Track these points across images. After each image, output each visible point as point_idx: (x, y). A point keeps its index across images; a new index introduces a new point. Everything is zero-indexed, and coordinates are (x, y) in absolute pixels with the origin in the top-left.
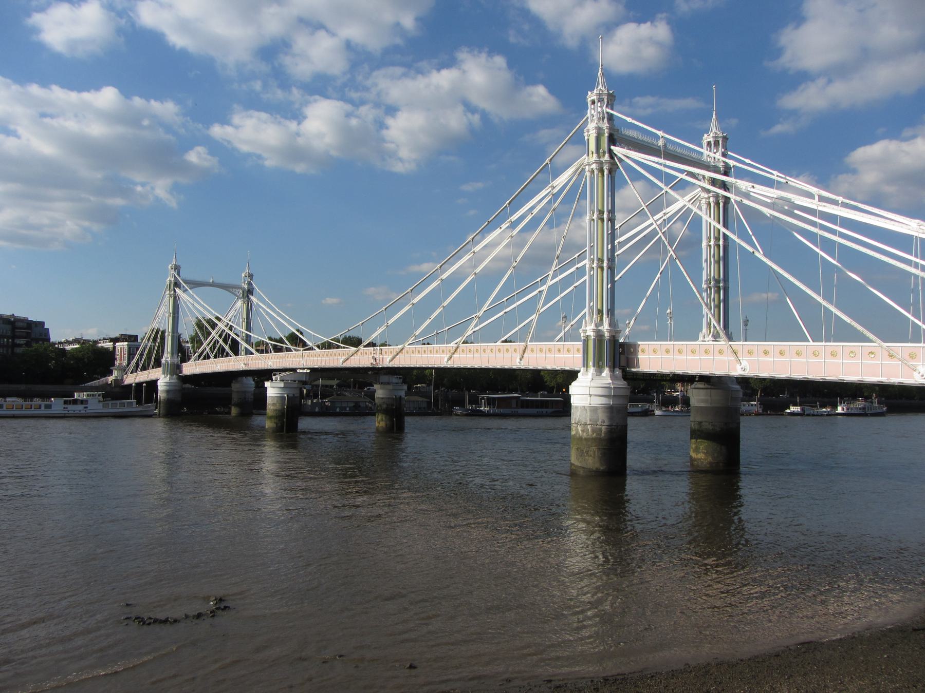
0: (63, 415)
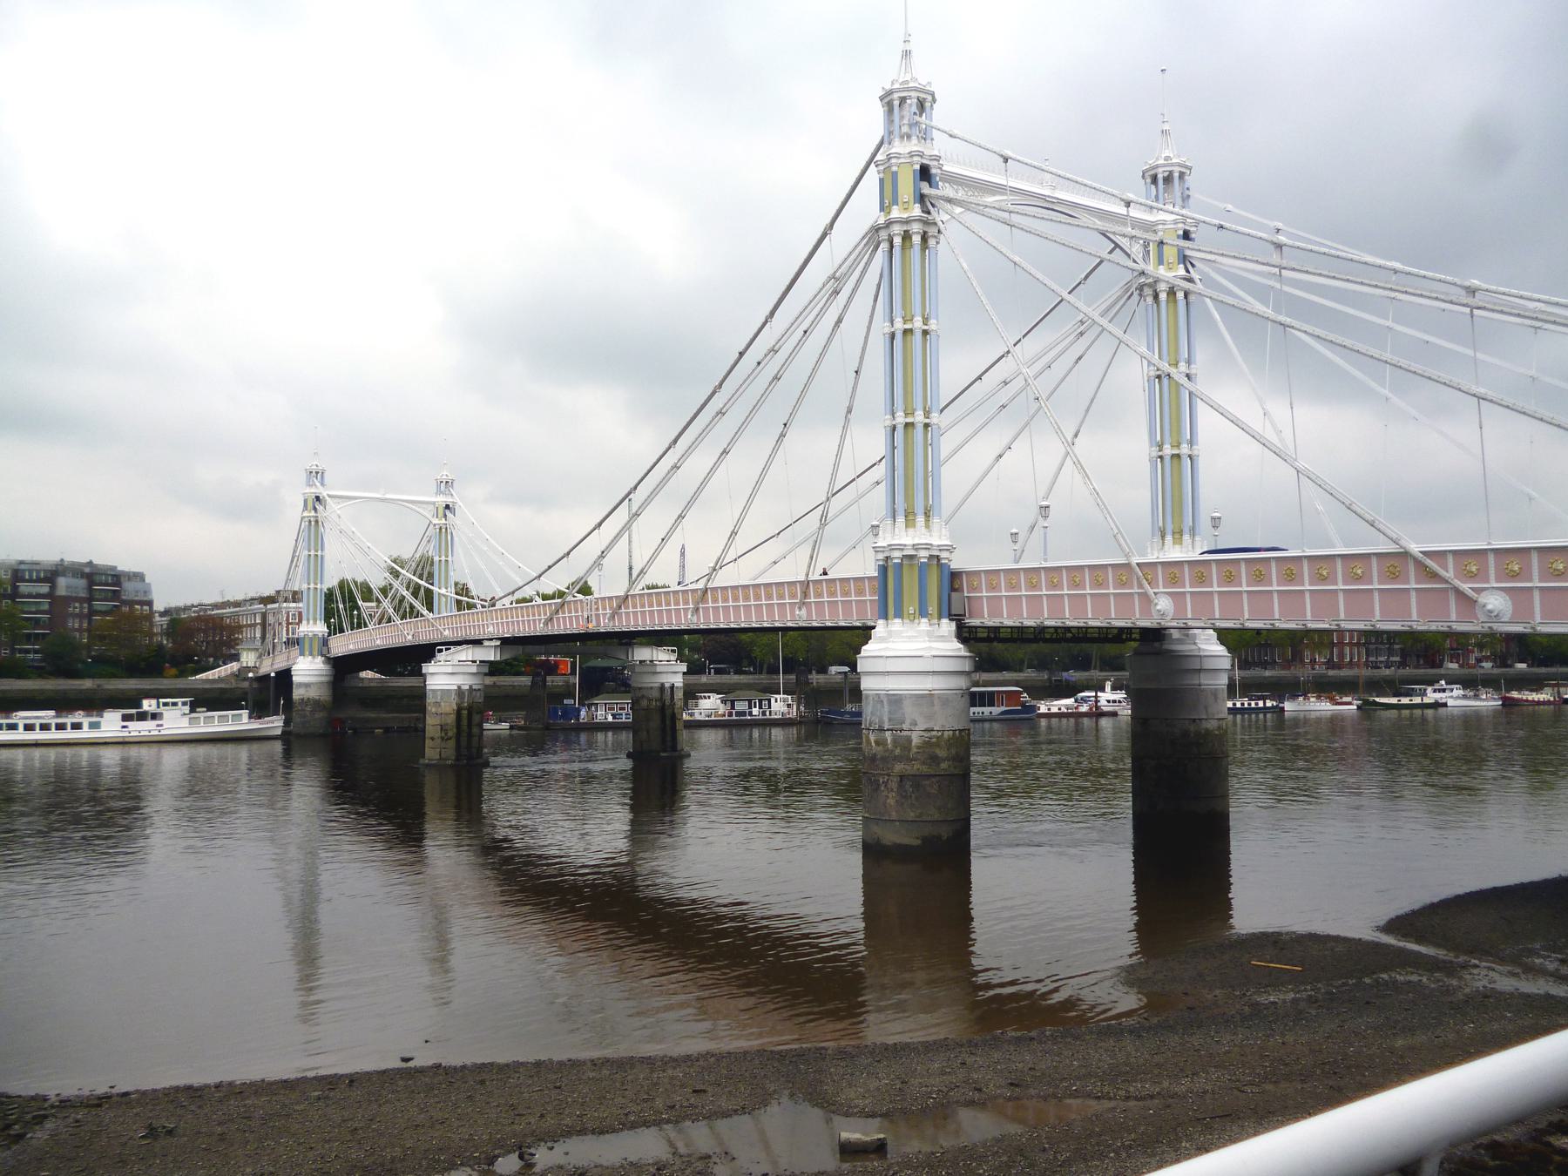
0: (121, 740)
